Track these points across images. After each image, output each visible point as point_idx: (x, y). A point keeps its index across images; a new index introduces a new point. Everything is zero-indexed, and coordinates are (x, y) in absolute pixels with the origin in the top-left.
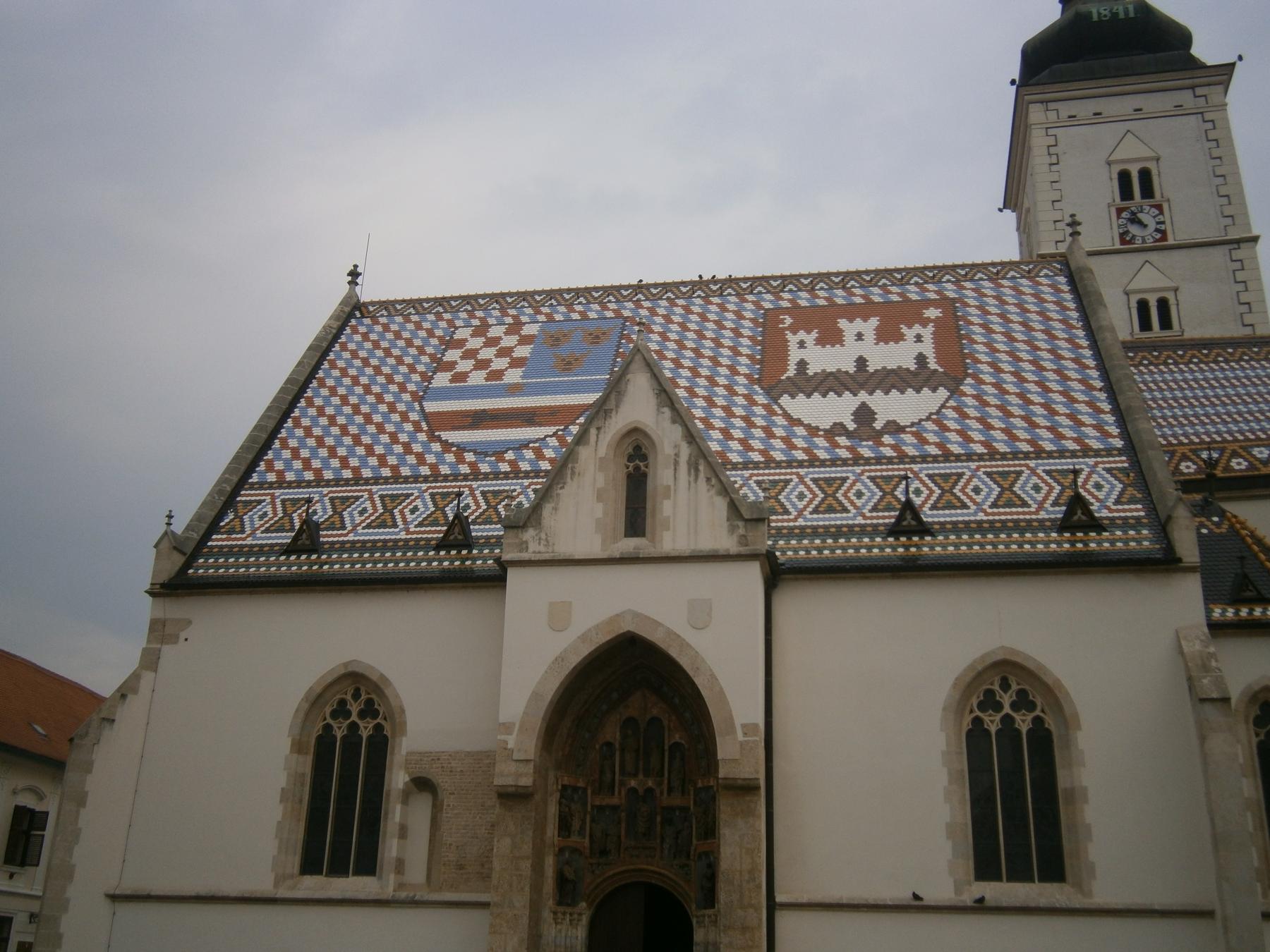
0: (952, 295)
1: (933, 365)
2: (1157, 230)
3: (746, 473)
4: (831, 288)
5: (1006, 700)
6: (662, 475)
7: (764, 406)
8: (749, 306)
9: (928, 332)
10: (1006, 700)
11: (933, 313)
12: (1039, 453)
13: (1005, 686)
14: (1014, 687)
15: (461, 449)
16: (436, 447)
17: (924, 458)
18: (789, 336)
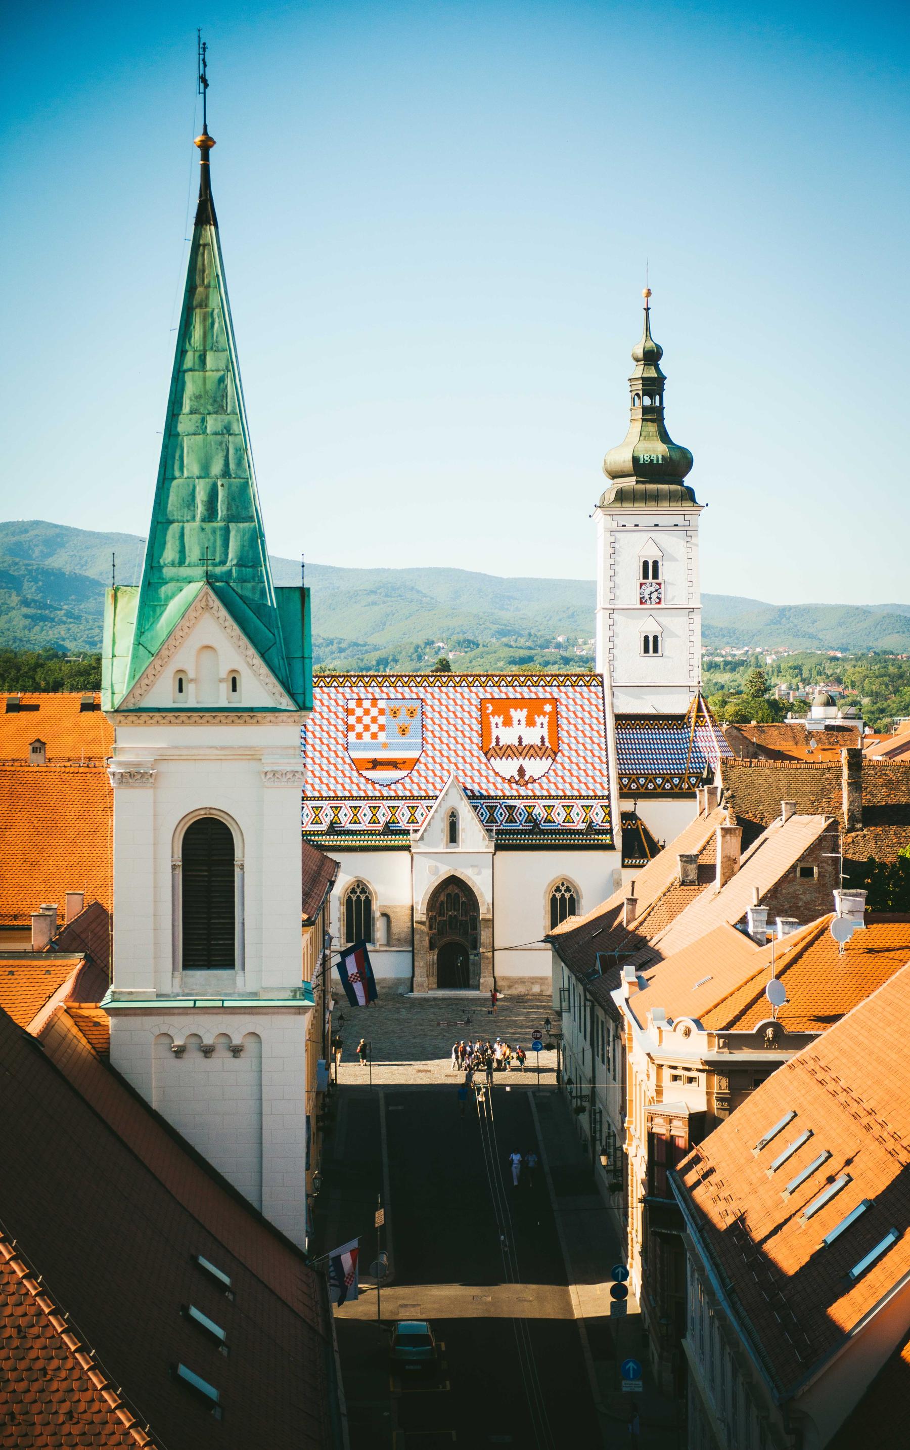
0: (556, 696)
1: (547, 744)
2: (658, 597)
3: (482, 801)
4: (507, 686)
5: (563, 889)
6: (461, 825)
7: (486, 764)
8: (473, 695)
9: (545, 720)
10: (563, 889)
11: (548, 708)
12: (581, 797)
13: (563, 884)
14: (565, 885)
15: (373, 783)
16: (363, 780)
17: (542, 797)
18: (492, 719)
